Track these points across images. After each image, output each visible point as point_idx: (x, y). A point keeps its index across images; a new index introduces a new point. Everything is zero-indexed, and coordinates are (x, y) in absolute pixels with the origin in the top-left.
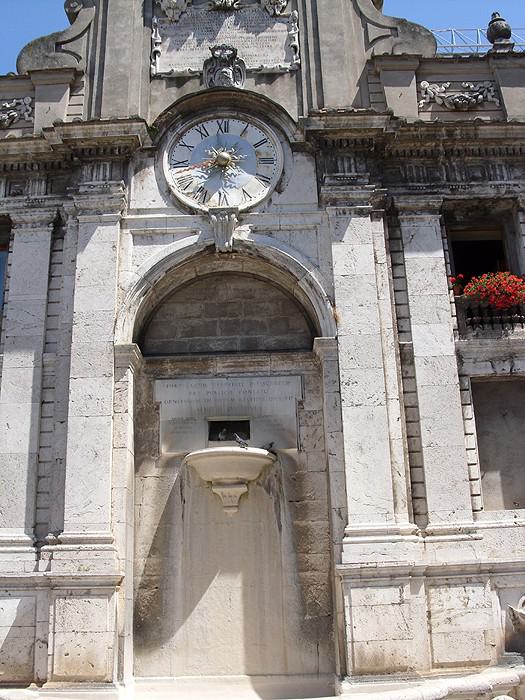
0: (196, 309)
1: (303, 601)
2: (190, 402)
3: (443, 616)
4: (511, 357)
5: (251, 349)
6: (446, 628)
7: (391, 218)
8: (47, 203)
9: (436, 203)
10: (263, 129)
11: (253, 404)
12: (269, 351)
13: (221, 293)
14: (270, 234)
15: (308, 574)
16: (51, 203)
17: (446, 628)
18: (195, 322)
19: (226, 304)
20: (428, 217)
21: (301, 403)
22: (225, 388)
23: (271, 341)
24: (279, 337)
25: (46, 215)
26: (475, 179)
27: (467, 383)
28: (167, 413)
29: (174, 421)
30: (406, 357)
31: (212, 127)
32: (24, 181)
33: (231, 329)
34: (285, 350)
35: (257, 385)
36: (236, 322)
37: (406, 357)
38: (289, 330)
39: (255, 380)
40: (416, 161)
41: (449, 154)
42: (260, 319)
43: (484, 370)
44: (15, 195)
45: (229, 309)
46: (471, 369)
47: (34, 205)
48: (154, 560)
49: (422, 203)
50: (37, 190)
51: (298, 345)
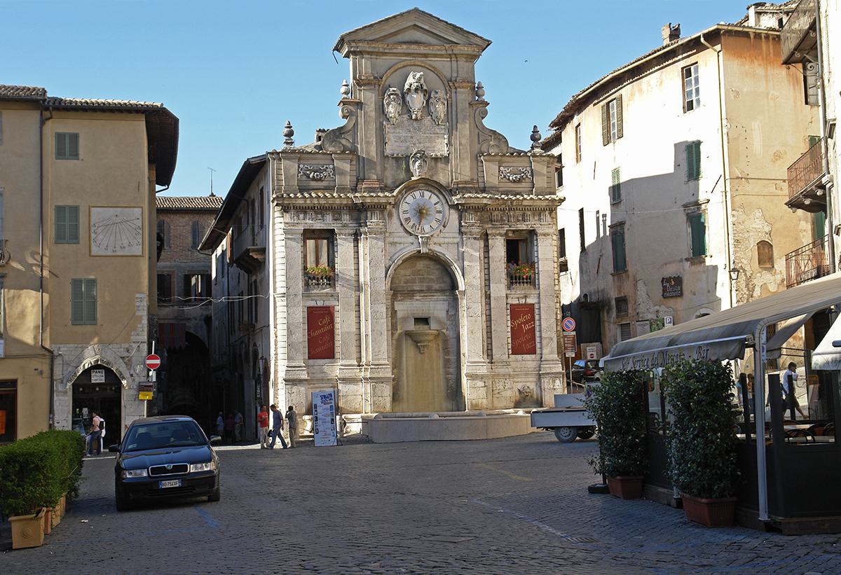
0: (408, 272)
1: (447, 386)
2: (407, 310)
3: (497, 391)
4: (526, 297)
5: (429, 290)
6: (498, 396)
7: (485, 237)
8: (350, 225)
9: (503, 232)
10: (438, 197)
11: (430, 312)
12: (437, 291)
13: (418, 265)
14: (440, 245)
15: (450, 376)
16: (350, 225)
17: (498, 396)
18: (408, 277)
19: (419, 271)
20: (499, 237)
21: (447, 312)
22: (420, 306)
23: (436, 286)
24: (441, 285)
25: (351, 232)
26: (519, 221)
27: (509, 306)
28: (400, 315)
29: (402, 318)
30: (488, 297)
31: (417, 194)
32: (340, 214)
33: (422, 281)
34: (442, 291)
35: (432, 305)
36: (424, 278)
37: (488, 297)
38: (445, 282)
39: (431, 302)
40: (497, 212)
41: (510, 210)
42: (432, 277)
43: (515, 302)
44: (336, 220)
45: (421, 272)
46: (510, 301)
47: (345, 226)
48: (395, 371)
49: (498, 232)
50: (346, 218)
51: (446, 288)
